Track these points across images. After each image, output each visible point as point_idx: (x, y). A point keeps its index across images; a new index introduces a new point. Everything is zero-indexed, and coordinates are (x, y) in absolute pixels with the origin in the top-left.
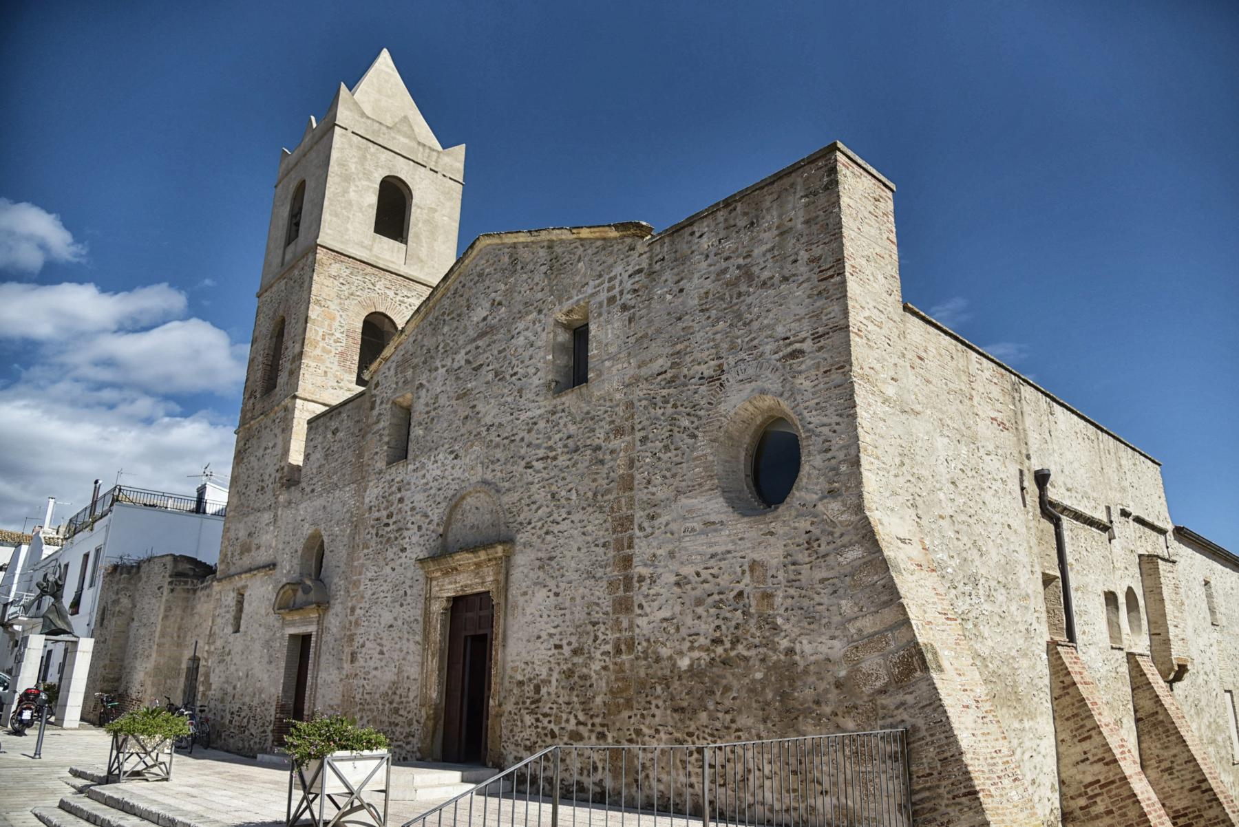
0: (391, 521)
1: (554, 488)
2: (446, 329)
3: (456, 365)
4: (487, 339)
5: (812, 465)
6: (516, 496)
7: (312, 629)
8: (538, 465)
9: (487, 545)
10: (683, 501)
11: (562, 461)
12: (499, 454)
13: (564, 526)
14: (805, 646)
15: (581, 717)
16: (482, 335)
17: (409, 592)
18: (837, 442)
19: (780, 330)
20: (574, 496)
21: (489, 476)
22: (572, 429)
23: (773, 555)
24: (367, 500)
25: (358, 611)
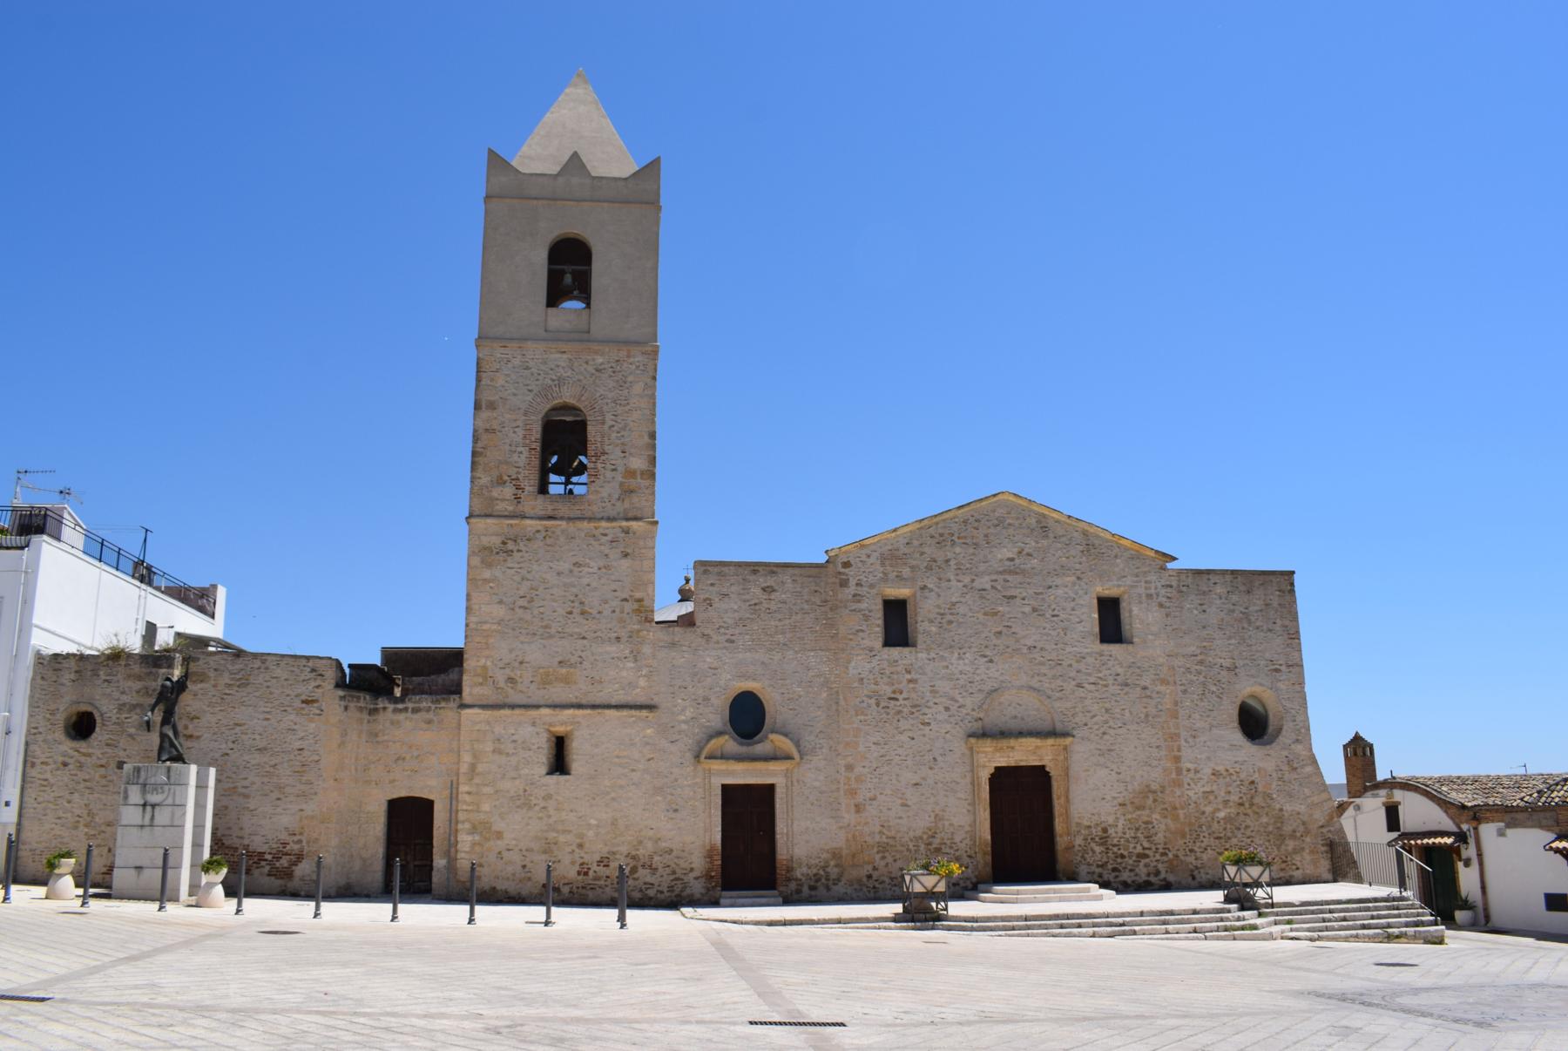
0: (900, 697)
1: (1108, 705)
2: (958, 550)
3: (977, 584)
4: (1019, 578)
5: (1288, 727)
6: (1069, 705)
7: (779, 781)
8: (1092, 687)
9: (1053, 734)
10: (1215, 731)
11: (1114, 689)
12: (1044, 670)
13: (1120, 731)
14: (1288, 807)
15: (1146, 845)
16: (1010, 572)
17: (939, 759)
18: (1299, 718)
19: (1267, 655)
20: (1127, 713)
21: (1034, 683)
22: (1120, 670)
23: (1270, 765)
24: (852, 671)
25: (858, 770)
